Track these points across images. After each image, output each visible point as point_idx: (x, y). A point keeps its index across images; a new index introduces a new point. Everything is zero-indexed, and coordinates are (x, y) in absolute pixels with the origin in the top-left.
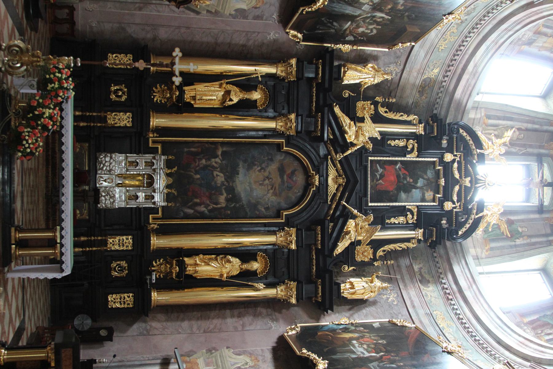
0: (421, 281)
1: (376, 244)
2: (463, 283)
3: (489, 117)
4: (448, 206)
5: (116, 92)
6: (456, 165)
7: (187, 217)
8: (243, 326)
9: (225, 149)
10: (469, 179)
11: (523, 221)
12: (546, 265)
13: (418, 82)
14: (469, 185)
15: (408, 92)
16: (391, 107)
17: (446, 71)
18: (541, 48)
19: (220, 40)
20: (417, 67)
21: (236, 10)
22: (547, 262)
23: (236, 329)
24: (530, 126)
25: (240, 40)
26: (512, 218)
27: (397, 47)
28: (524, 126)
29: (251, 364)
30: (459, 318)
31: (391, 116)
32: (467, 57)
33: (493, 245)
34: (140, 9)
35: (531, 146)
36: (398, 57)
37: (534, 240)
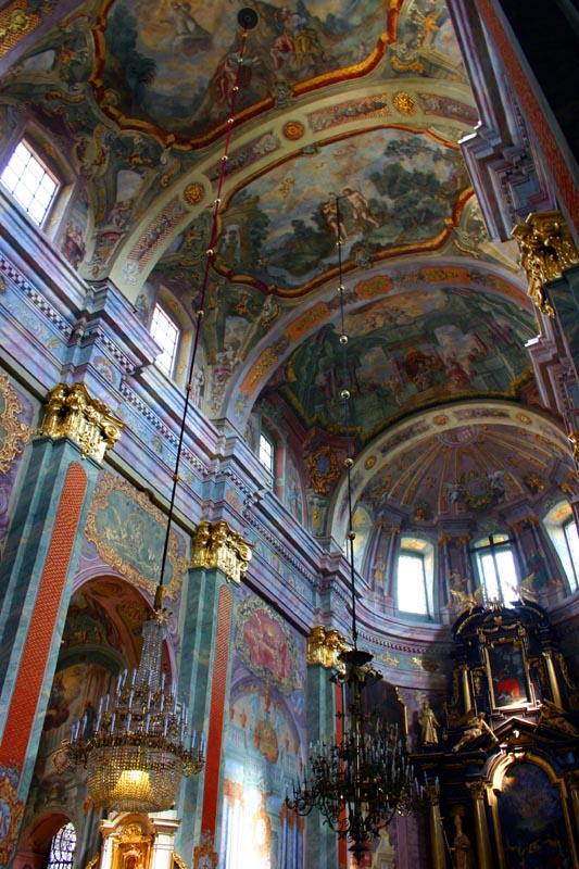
3: (446, 602)
4: (522, 631)
6: (488, 631)
9: (508, 843)
12: (557, 526)
13: (426, 674)
15: (436, 680)
16: (451, 693)
19: (417, 855)
21: (391, 845)
22: (555, 526)
24: (447, 566)
25: (414, 837)
27: (403, 702)
28: (447, 571)
31: (457, 695)
33: (551, 577)
35: (463, 560)
37: (539, 543)
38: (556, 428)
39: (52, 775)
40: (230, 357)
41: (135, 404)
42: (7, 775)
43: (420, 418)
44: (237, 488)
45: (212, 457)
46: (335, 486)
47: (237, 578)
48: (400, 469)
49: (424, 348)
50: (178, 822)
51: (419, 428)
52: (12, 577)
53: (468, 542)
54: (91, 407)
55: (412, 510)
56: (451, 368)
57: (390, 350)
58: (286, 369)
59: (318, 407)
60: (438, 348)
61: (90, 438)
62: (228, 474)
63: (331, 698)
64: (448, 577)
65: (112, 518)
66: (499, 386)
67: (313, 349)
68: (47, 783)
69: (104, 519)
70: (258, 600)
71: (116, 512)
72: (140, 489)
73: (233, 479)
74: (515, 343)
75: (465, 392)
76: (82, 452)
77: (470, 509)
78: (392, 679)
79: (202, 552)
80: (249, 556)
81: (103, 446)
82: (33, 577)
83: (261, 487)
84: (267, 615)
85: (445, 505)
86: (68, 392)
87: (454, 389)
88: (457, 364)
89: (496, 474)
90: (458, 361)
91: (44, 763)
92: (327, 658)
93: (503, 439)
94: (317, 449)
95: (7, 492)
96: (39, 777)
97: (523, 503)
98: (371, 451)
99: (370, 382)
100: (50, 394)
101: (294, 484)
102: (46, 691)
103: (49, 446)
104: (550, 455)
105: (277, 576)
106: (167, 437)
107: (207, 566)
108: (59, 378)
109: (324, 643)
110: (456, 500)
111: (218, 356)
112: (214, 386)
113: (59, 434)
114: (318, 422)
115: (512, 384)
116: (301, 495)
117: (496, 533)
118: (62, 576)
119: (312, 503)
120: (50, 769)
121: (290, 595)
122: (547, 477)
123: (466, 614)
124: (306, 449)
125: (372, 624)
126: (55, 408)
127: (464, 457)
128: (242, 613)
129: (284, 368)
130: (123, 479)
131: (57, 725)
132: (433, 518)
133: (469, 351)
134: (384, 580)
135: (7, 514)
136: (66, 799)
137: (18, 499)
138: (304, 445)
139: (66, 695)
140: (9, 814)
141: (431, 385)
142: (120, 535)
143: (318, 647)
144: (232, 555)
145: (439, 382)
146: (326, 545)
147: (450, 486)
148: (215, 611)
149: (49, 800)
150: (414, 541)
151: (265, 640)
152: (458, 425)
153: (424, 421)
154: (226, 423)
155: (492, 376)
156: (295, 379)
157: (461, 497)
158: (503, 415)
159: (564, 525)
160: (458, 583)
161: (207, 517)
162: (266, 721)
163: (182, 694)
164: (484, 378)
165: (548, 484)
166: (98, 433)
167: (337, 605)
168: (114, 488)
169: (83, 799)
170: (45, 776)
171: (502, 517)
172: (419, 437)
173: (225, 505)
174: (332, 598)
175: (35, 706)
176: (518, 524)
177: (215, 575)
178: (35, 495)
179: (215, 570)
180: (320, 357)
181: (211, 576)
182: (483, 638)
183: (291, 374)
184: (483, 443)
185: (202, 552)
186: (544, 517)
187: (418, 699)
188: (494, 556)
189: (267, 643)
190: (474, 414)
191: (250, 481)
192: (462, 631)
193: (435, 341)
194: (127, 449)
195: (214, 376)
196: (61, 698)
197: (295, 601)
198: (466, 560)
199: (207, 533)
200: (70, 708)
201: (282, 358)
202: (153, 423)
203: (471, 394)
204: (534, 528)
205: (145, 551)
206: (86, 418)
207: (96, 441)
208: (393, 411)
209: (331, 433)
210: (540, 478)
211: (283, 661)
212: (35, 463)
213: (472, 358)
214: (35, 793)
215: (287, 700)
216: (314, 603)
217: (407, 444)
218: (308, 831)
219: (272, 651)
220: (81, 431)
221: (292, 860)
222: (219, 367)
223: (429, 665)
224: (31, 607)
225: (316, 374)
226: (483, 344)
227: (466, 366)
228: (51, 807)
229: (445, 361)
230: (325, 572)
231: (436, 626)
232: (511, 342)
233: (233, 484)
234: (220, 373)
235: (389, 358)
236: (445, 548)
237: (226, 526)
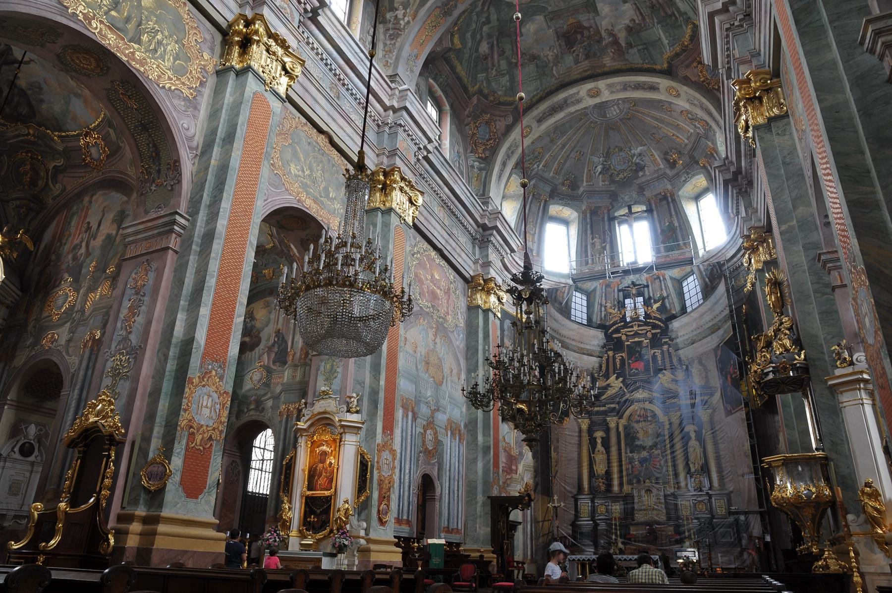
3: (587, 263)
11: (660, 223)
18: (533, 242)
24: (589, 232)
26: (659, 231)
28: (589, 236)
35: (604, 227)
37: (673, 213)
38: (704, 100)
39: (250, 390)
40: (400, 16)
41: (313, 49)
42: (213, 368)
43: (572, 91)
44: (409, 139)
45: (386, 109)
46: (494, 151)
47: (409, 220)
48: (552, 141)
49: (584, 18)
50: (363, 423)
51: (573, 100)
52: (205, 195)
53: (609, 210)
54: (271, 40)
55: (560, 181)
56: (607, 40)
57: (551, 20)
58: (452, 35)
59: (481, 76)
60: (597, 18)
61: (273, 71)
62: (400, 125)
63: (488, 335)
64: (590, 241)
65: (295, 154)
66: (652, 59)
67: (478, 15)
68: (245, 397)
69: (288, 155)
70: (426, 245)
71: (299, 149)
72: (320, 131)
73: (405, 131)
74: (673, 13)
75: (618, 65)
76: (265, 83)
77: (612, 181)
79: (378, 195)
80: (420, 201)
81: (284, 80)
82: (225, 194)
83: (430, 141)
84: (433, 260)
85: (590, 178)
86: (248, 23)
87: (608, 62)
88: (614, 36)
90: (616, 32)
91: (242, 381)
92: (485, 302)
93: (648, 116)
94: (479, 117)
95: (194, 116)
96: (238, 391)
97: (662, 176)
98: (527, 120)
99: (531, 52)
100: (230, 26)
101: (457, 148)
102: (239, 320)
103: (232, 75)
104: (692, 131)
105: (443, 226)
106: (344, 85)
107: (382, 206)
108: (237, 10)
109: (483, 289)
110: (600, 173)
111: (389, 15)
112: (385, 45)
113: (241, 65)
114: (480, 92)
115: (666, 57)
116: (463, 157)
117: (635, 204)
118: (252, 198)
119: (473, 167)
120: (248, 385)
121: (454, 244)
124: (468, 117)
126: (237, 39)
128: (413, 255)
129: (450, 33)
130: (304, 120)
131: (252, 349)
132: (579, 188)
133: (627, 22)
134: (533, 242)
135: (196, 138)
136: (263, 409)
137: (205, 125)
138: (466, 113)
139: (258, 325)
140: (217, 401)
141: (587, 57)
142: (303, 171)
143: (477, 291)
144: (405, 199)
145: (595, 54)
146: (486, 203)
147: (596, 160)
148: (391, 246)
149: (249, 410)
150: (561, 208)
151: (432, 282)
152: (610, 99)
153: (578, 93)
154: (398, 79)
155: (646, 49)
156: (459, 46)
157: (606, 170)
159: (697, 198)
160: (598, 247)
162: (433, 350)
164: (639, 50)
165: (688, 160)
166: (279, 68)
167: (493, 257)
168: (296, 128)
169: (279, 407)
170: (244, 390)
171: (641, 189)
172: (572, 109)
173: (399, 153)
174: (490, 251)
175: (234, 311)
176: (655, 196)
177: (390, 215)
178: (222, 121)
179: (391, 210)
180: (484, 24)
181: (386, 216)
183: (456, 40)
184: (629, 119)
185: (378, 195)
186: (680, 189)
188: (631, 226)
189: (435, 285)
190: (625, 87)
191: (420, 134)
193: (596, 11)
194: (307, 91)
195: (385, 36)
196: (253, 327)
197: (458, 250)
198: (607, 227)
199: (382, 178)
200: (261, 335)
201: (450, 20)
202: (331, 70)
203: (624, 67)
204: (670, 200)
205: (326, 189)
206: (268, 51)
207: (278, 75)
208: (552, 82)
209: (492, 101)
210: (680, 153)
211: (448, 301)
212: (218, 91)
213: (629, 29)
214: (236, 405)
215: (451, 336)
216: (474, 254)
217: (560, 115)
218: (467, 443)
219: (438, 291)
220: (263, 63)
221: (455, 463)
222: (390, 26)
224: (225, 223)
225: (480, 41)
226: (641, 14)
227: (622, 37)
228: (251, 415)
229: (603, 34)
230: (484, 227)
232: (669, 12)
233: (405, 135)
234: (391, 32)
235: (549, 27)
236: (588, 215)
237: (400, 172)
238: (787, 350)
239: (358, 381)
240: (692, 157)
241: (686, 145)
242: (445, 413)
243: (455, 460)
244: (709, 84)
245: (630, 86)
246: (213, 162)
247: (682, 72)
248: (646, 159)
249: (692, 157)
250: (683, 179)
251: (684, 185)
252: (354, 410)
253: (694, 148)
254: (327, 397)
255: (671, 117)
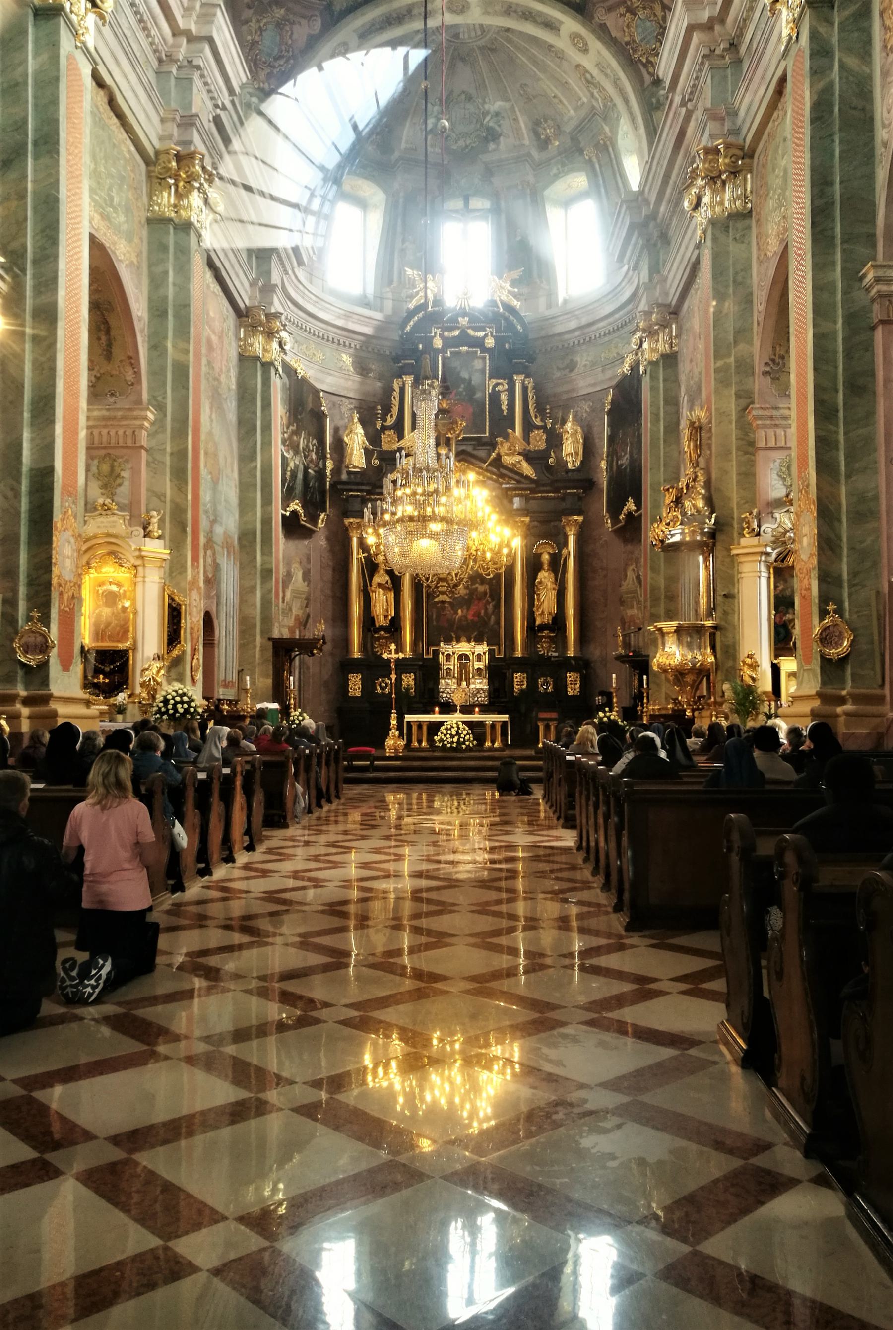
0: (571, 371)
1: (528, 427)
2: (573, 324)
3: (391, 282)
4: (490, 342)
5: (382, 689)
7: (498, 622)
8: (602, 569)
10: (460, 319)
13: (358, 378)
14: (467, 319)
16: (387, 410)
17: (345, 346)
19: (329, 592)
20: (342, 382)
23: (605, 576)
24: (399, 229)
25: (329, 574)
27: (326, 412)
29: (633, 566)
30: (609, 333)
31: (395, 410)
32: (330, 328)
34: (308, 668)
36: (334, 404)
38: (622, 75)
45: (176, 32)
62: (198, 68)
78: (317, 380)
89: (498, 105)
92: (265, 350)
104: (585, 100)
122: (568, 129)
123: (423, 307)
125: (300, 301)
127: (460, 64)
158: (550, 25)
159: (567, 203)
161: (170, 137)
163: (154, 397)
181: (182, 235)
182: (438, 343)
186: (545, 187)
187: (344, 409)
192: (412, 328)
223: (362, 368)
231: (378, 316)
236: (401, 200)
237: (202, 160)
238: (698, 511)
239: (154, 492)
240: (575, 140)
241: (571, 118)
242: (221, 524)
243: (231, 589)
244: (635, 51)
245: (515, 12)
246: (30, 186)
247: (600, 15)
248: (506, 126)
249: (575, 140)
250: (555, 171)
251: (553, 182)
252: (156, 535)
253: (580, 128)
254: (109, 512)
255: (559, 67)
